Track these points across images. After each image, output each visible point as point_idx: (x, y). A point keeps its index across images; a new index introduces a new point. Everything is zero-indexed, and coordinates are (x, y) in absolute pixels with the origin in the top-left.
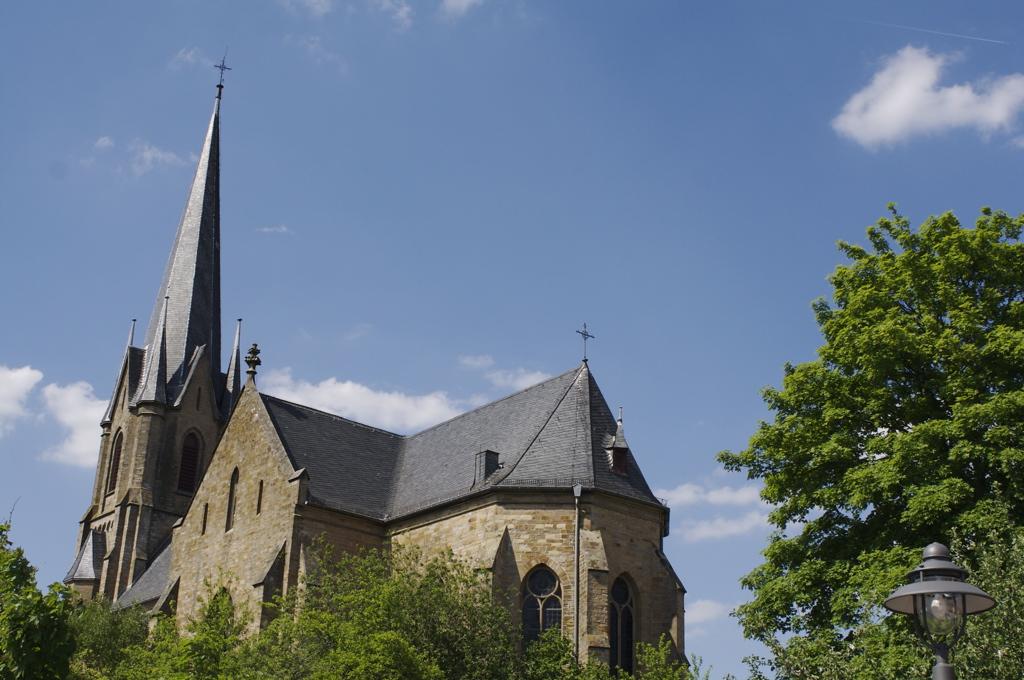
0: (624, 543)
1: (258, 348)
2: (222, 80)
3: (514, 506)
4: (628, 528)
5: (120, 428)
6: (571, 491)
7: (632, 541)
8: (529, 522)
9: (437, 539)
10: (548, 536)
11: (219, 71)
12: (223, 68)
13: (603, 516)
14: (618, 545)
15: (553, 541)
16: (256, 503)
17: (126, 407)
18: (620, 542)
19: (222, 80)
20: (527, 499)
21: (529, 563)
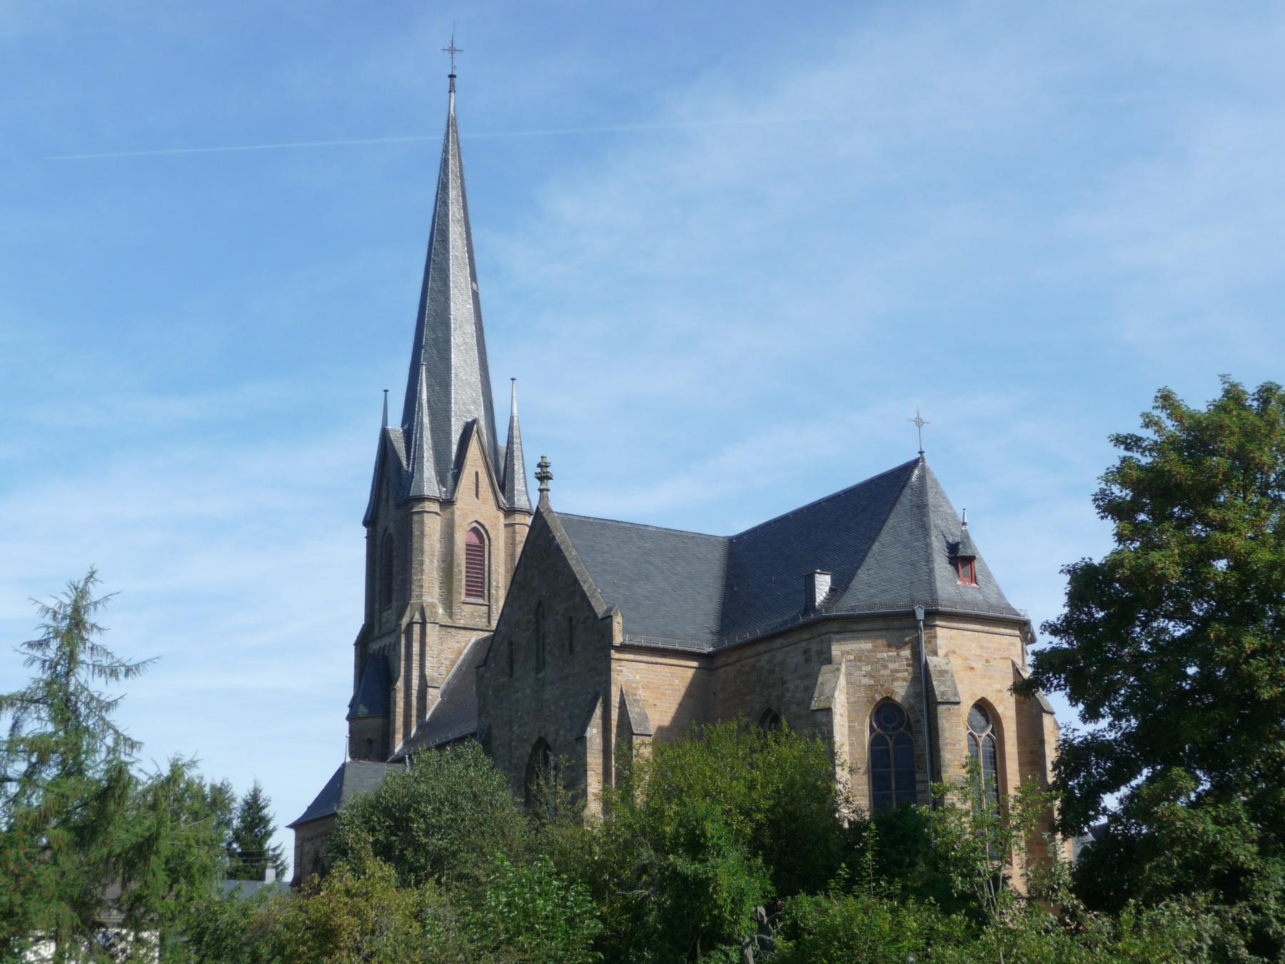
0: (978, 665)
1: (548, 460)
2: (453, 67)
3: (850, 634)
4: (982, 647)
5: (387, 529)
6: (912, 614)
7: (987, 661)
8: (868, 651)
9: (772, 672)
10: (891, 666)
11: (448, 55)
12: (452, 50)
13: (952, 638)
14: (972, 669)
15: (897, 671)
16: (566, 642)
17: (392, 504)
18: (974, 665)
19: (453, 67)
20: (865, 626)
21: (873, 698)
